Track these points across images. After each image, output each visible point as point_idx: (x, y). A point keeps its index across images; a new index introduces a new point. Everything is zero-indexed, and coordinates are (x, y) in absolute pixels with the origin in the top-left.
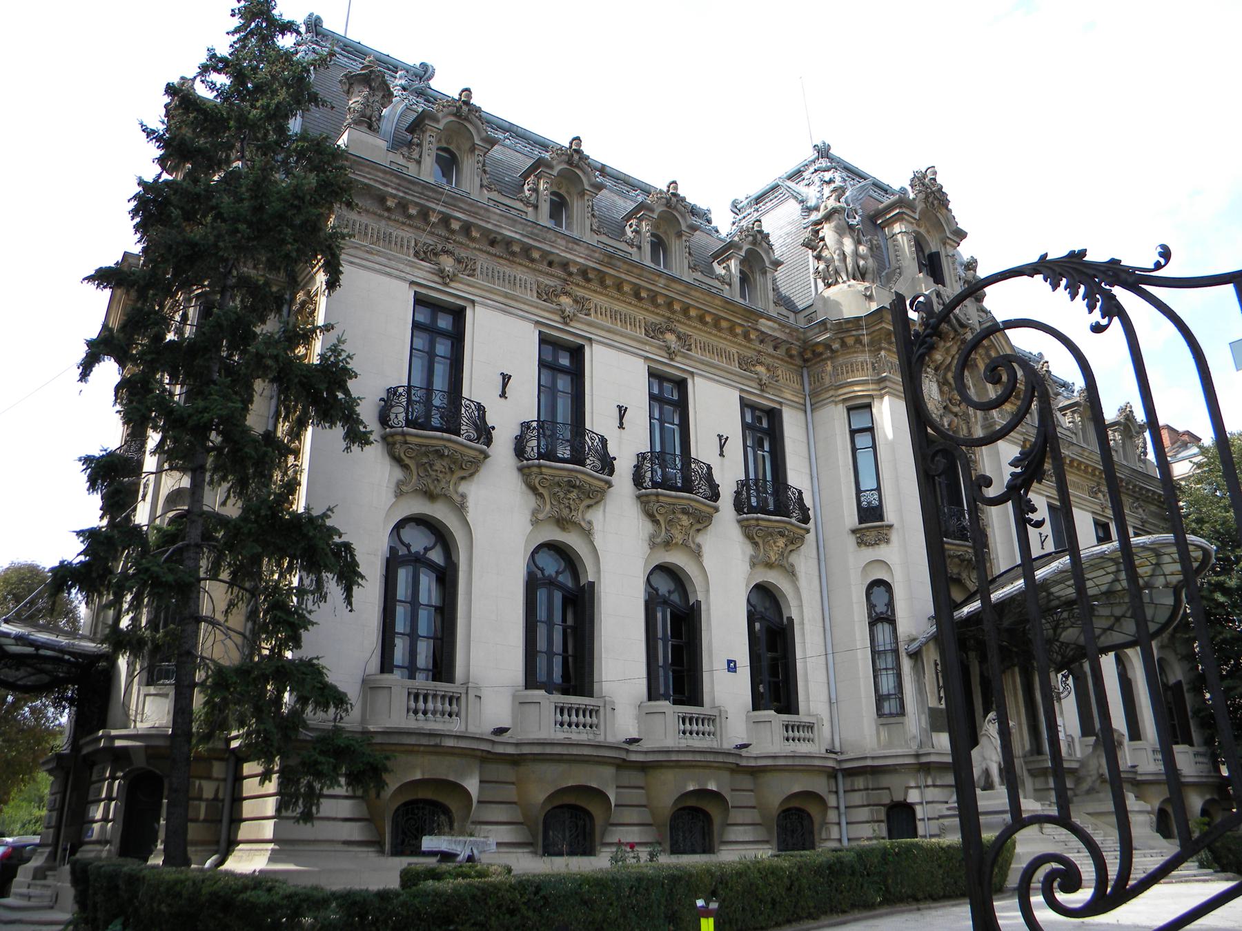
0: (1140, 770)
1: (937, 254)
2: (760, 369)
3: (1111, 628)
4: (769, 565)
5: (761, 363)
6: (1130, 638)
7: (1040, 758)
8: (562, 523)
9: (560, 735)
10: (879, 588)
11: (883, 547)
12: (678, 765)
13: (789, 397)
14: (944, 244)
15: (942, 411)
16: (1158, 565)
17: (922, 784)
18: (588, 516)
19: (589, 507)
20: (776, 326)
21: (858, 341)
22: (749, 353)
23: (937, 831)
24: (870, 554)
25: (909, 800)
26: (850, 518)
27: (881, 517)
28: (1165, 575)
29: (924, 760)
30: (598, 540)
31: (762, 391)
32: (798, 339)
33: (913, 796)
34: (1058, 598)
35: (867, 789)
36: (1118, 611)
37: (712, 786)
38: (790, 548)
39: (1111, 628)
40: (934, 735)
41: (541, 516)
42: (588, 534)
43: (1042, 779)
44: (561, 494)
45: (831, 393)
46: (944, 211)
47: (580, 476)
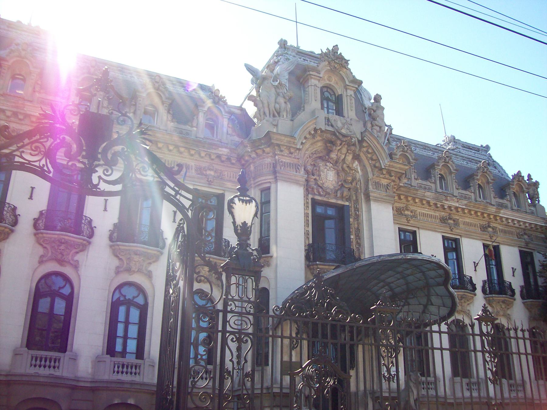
1: (341, 95)
2: (209, 172)
5: (210, 169)
8: (61, 262)
9: (32, 371)
12: (107, 389)
13: (230, 187)
14: (346, 89)
18: (76, 258)
19: (77, 253)
21: (264, 151)
22: (204, 165)
27: (269, 253)
30: (83, 271)
37: (131, 401)
41: (44, 259)
42: (76, 266)
44: (56, 247)
46: (345, 70)
47: (64, 237)
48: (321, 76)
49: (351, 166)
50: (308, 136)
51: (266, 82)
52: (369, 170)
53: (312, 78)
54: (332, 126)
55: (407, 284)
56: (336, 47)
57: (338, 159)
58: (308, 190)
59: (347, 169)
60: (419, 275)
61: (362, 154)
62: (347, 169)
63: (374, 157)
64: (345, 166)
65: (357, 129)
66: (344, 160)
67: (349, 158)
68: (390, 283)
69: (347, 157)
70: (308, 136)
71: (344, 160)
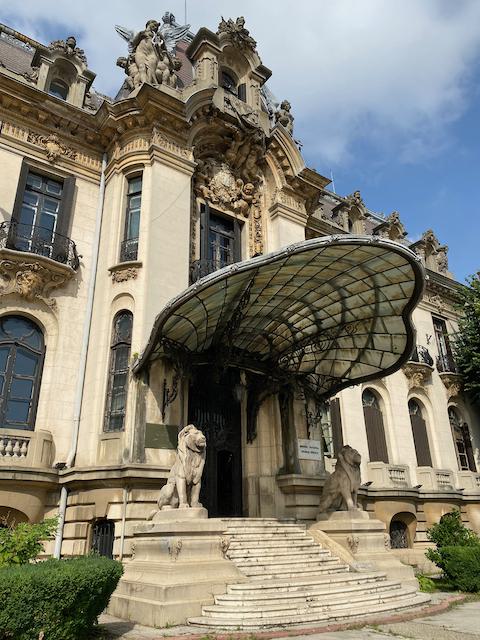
0: (421, 490)
3: (357, 361)
4: (24, 298)
6: (378, 370)
7: (289, 476)
10: (124, 318)
11: (131, 282)
15: (235, 197)
16: (376, 288)
17: (124, 500)
20: (66, 110)
23: (127, 551)
24: (121, 288)
25: (108, 518)
26: (112, 258)
28: (387, 300)
29: (128, 474)
31: (51, 162)
32: (93, 126)
33: (114, 513)
34: (300, 329)
35: (79, 504)
36: (361, 343)
38: (51, 284)
39: (357, 361)
40: (149, 452)
43: (292, 496)
45: (116, 166)
48: (221, 50)
49: (253, 172)
50: (201, 113)
51: (143, 41)
52: (278, 179)
53: (207, 50)
54: (233, 109)
55: (344, 310)
56: (241, 21)
57: (237, 161)
58: (196, 193)
59: (247, 176)
60: (368, 295)
61: (268, 159)
62: (247, 176)
63: (285, 163)
64: (245, 172)
65: (267, 126)
66: (244, 164)
67: (252, 161)
68: (320, 309)
69: (249, 160)
70: (201, 113)
71: (244, 164)
